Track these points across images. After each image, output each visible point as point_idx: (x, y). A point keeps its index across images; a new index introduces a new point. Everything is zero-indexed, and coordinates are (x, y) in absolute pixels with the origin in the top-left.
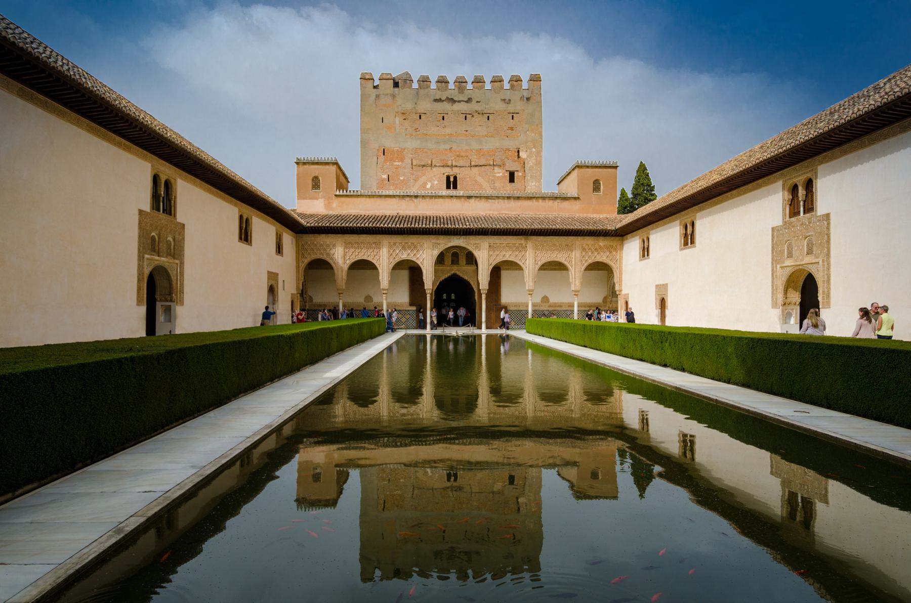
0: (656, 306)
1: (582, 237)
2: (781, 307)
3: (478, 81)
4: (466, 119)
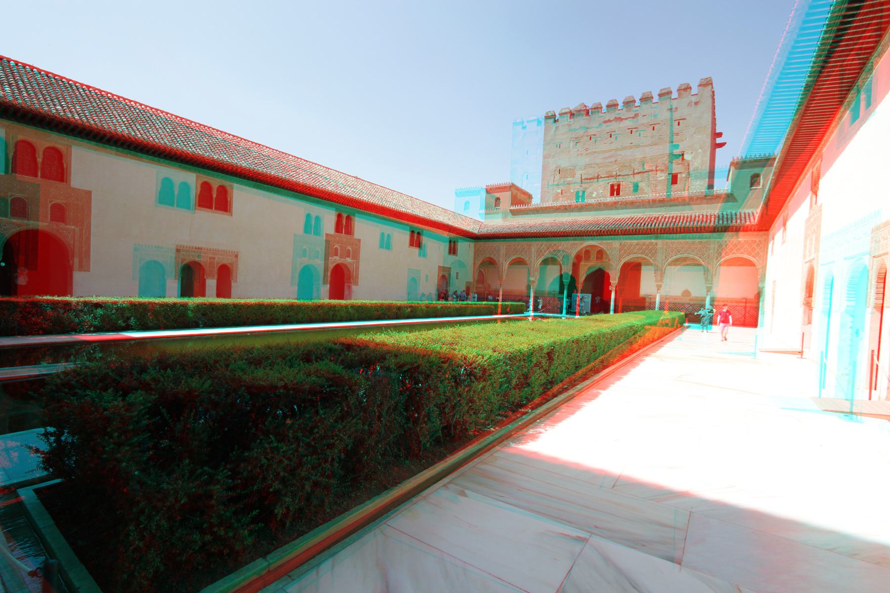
2: (803, 306)
3: (646, 99)
4: (631, 133)
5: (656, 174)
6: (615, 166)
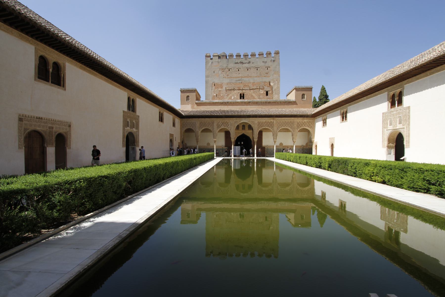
0: (329, 147)
1: (297, 118)
2: (386, 148)
3: (253, 55)
4: (248, 70)
5: (260, 90)
6: (241, 85)
